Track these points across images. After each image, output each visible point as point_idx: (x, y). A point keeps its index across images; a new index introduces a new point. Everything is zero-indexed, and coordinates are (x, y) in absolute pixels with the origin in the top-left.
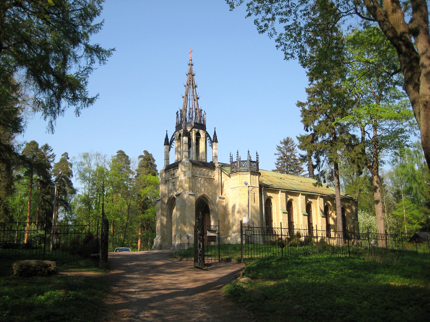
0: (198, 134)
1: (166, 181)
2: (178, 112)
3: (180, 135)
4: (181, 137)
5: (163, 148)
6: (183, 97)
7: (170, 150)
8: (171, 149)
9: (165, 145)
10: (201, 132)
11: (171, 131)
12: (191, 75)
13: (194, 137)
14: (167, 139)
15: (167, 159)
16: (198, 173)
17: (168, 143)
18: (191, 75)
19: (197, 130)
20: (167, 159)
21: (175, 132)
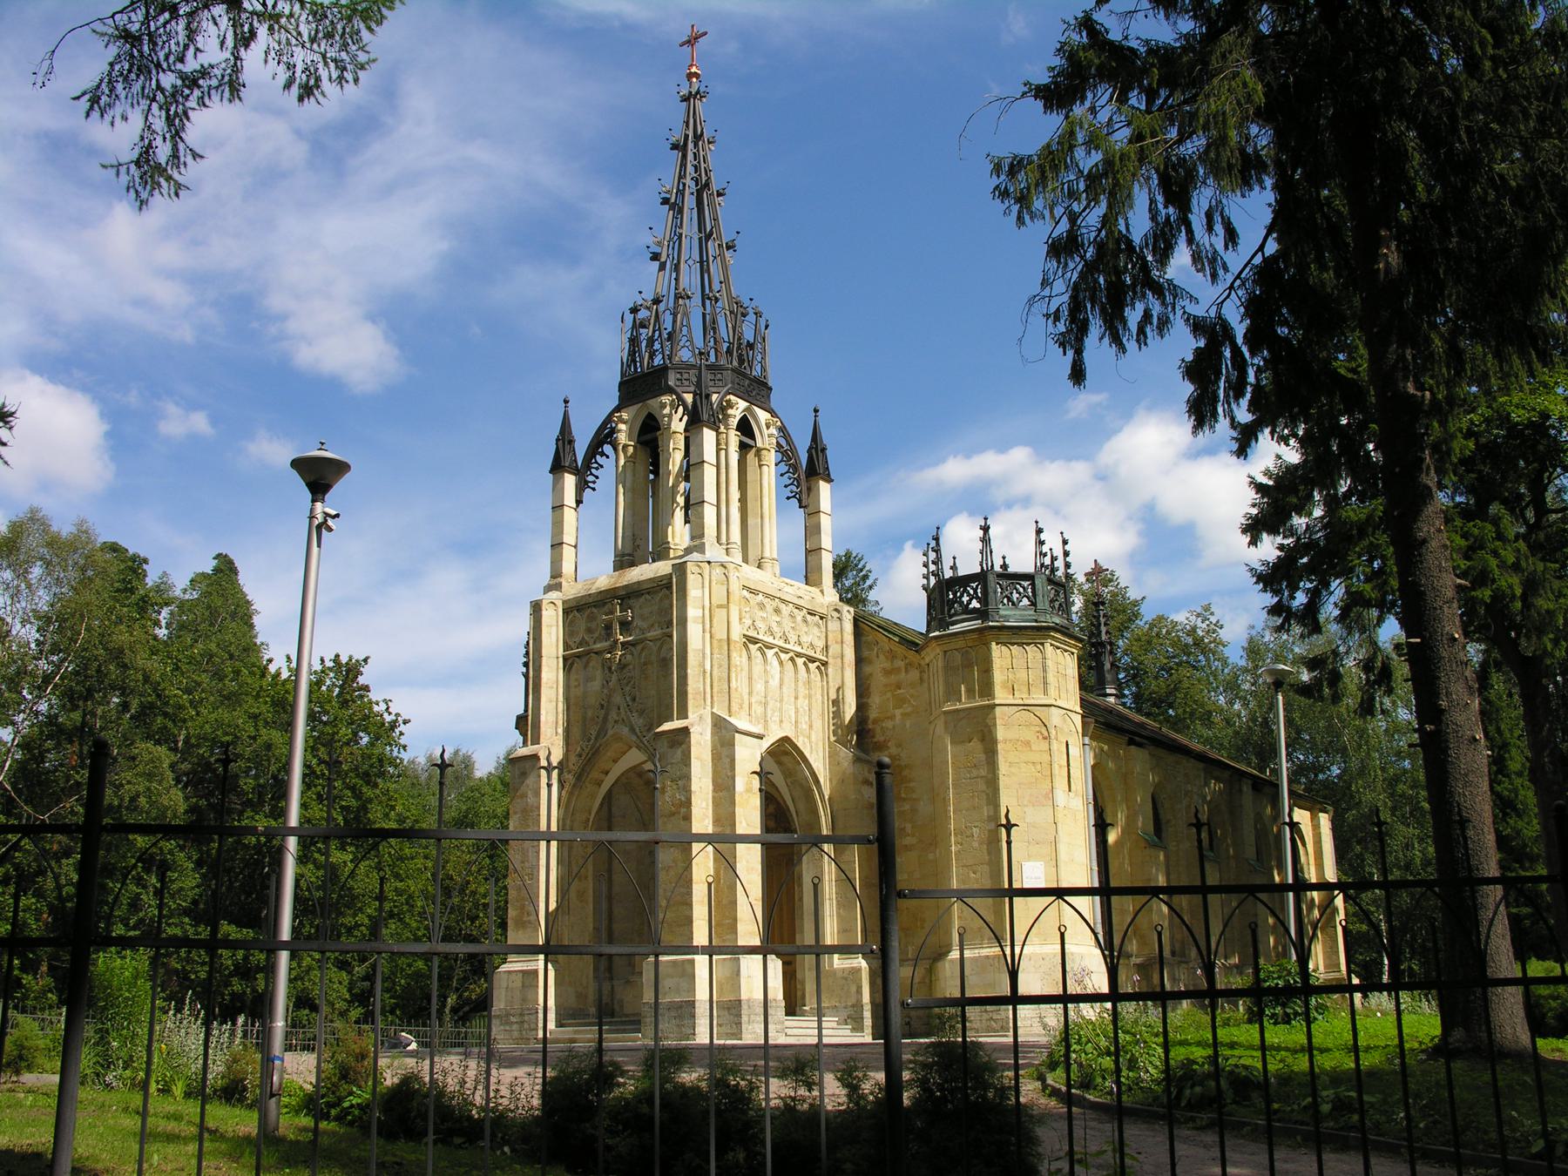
0: (745, 427)
14: (565, 438)
19: (743, 404)
21: (618, 409)
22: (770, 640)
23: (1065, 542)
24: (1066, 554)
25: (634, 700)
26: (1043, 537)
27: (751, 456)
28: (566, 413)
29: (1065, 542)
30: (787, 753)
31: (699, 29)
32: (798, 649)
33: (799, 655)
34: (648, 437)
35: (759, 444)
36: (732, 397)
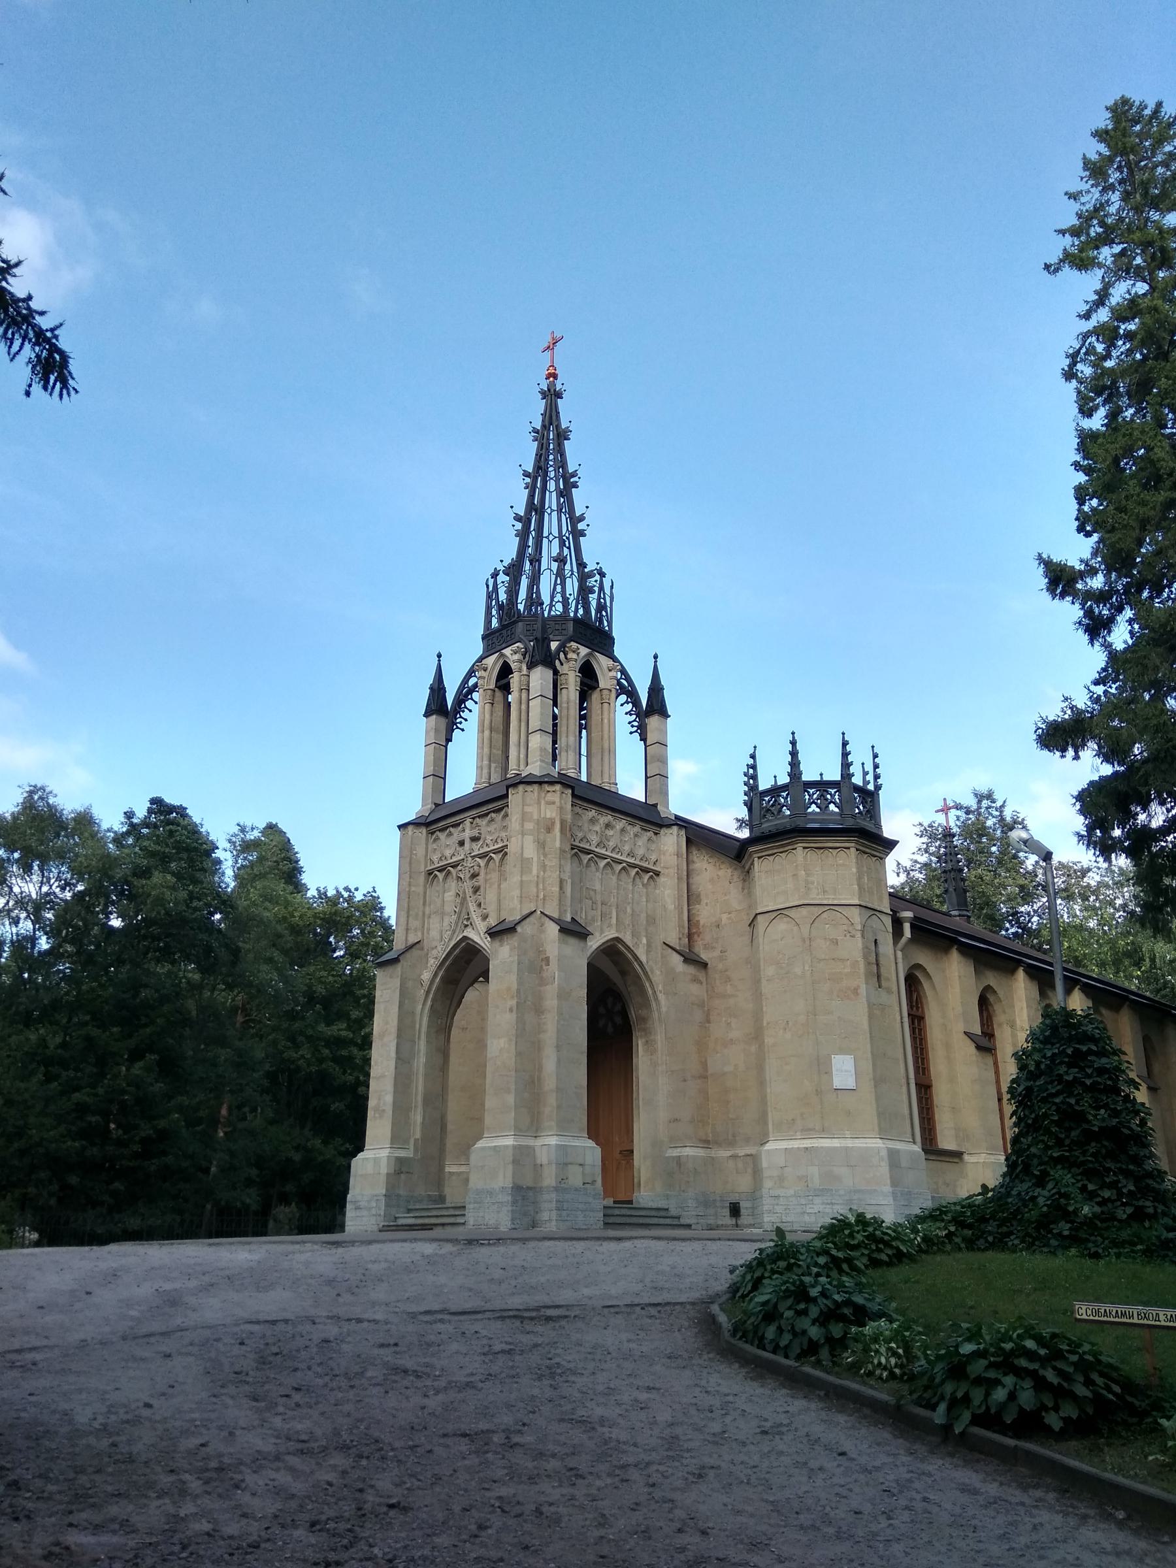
1: (430, 873)
2: (495, 575)
3: (506, 670)
4: (515, 680)
5: (418, 728)
6: (518, 518)
7: (449, 740)
8: (456, 733)
9: (427, 715)
10: (602, 663)
11: (463, 650)
12: (551, 436)
13: (572, 681)
14: (438, 689)
15: (438, 775)
16: (595, 839)
17: (443, 709)
18: (551, 436)
19: (584, 651)
20: (438, 775)
21: (481, 659)
22: (603, 851)
23: (875, 756)
24: (876, 766)
25: (479, 905)
26: (848, 748)
27: (595, 696)
28: (439, 667)
29: (875, 756)
30: (620, 953)
31: (558, 335)
32: (632, 861)
33: (634, 866)
34: (504, 681)
35: (602, 685)
36: (574, 645)
